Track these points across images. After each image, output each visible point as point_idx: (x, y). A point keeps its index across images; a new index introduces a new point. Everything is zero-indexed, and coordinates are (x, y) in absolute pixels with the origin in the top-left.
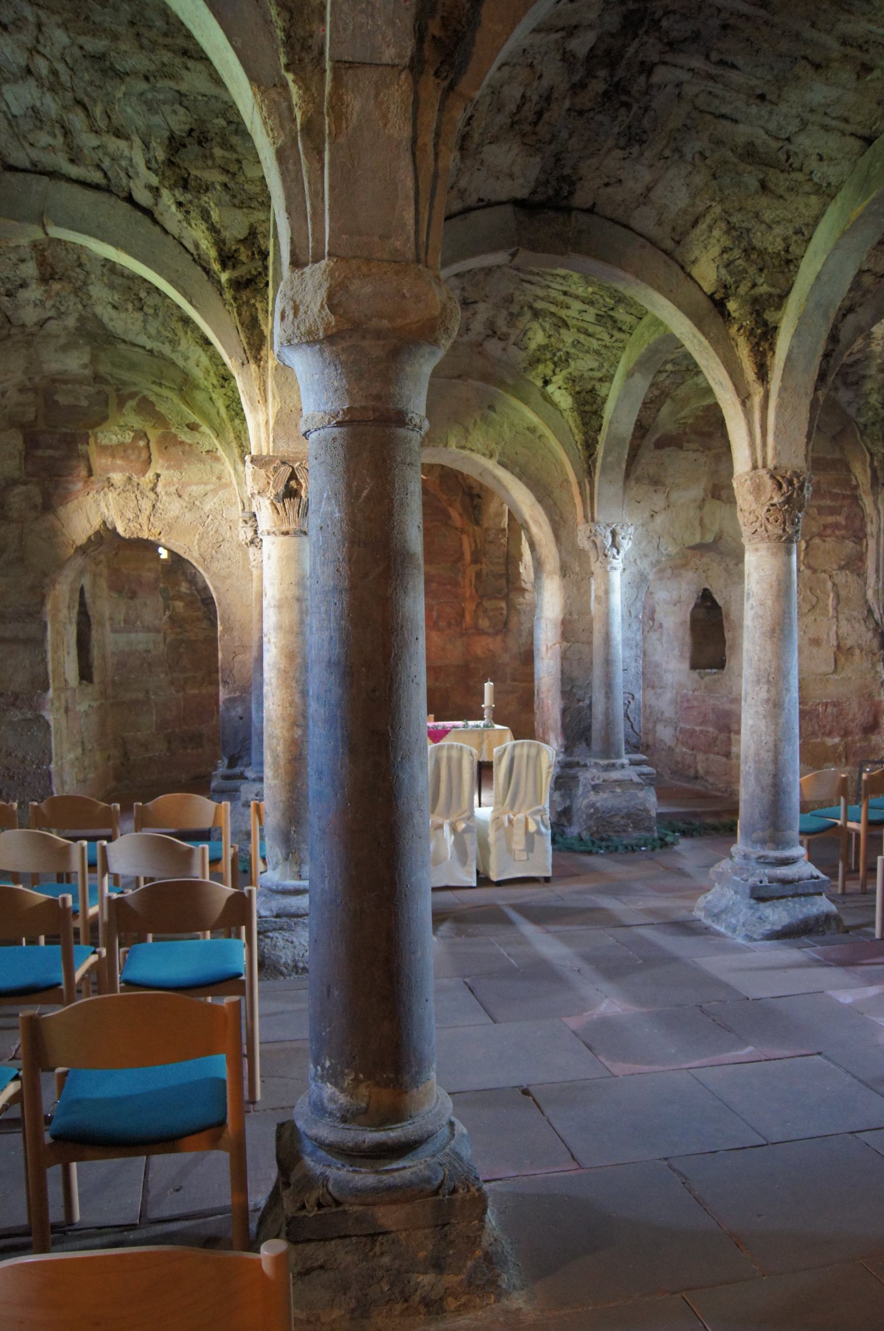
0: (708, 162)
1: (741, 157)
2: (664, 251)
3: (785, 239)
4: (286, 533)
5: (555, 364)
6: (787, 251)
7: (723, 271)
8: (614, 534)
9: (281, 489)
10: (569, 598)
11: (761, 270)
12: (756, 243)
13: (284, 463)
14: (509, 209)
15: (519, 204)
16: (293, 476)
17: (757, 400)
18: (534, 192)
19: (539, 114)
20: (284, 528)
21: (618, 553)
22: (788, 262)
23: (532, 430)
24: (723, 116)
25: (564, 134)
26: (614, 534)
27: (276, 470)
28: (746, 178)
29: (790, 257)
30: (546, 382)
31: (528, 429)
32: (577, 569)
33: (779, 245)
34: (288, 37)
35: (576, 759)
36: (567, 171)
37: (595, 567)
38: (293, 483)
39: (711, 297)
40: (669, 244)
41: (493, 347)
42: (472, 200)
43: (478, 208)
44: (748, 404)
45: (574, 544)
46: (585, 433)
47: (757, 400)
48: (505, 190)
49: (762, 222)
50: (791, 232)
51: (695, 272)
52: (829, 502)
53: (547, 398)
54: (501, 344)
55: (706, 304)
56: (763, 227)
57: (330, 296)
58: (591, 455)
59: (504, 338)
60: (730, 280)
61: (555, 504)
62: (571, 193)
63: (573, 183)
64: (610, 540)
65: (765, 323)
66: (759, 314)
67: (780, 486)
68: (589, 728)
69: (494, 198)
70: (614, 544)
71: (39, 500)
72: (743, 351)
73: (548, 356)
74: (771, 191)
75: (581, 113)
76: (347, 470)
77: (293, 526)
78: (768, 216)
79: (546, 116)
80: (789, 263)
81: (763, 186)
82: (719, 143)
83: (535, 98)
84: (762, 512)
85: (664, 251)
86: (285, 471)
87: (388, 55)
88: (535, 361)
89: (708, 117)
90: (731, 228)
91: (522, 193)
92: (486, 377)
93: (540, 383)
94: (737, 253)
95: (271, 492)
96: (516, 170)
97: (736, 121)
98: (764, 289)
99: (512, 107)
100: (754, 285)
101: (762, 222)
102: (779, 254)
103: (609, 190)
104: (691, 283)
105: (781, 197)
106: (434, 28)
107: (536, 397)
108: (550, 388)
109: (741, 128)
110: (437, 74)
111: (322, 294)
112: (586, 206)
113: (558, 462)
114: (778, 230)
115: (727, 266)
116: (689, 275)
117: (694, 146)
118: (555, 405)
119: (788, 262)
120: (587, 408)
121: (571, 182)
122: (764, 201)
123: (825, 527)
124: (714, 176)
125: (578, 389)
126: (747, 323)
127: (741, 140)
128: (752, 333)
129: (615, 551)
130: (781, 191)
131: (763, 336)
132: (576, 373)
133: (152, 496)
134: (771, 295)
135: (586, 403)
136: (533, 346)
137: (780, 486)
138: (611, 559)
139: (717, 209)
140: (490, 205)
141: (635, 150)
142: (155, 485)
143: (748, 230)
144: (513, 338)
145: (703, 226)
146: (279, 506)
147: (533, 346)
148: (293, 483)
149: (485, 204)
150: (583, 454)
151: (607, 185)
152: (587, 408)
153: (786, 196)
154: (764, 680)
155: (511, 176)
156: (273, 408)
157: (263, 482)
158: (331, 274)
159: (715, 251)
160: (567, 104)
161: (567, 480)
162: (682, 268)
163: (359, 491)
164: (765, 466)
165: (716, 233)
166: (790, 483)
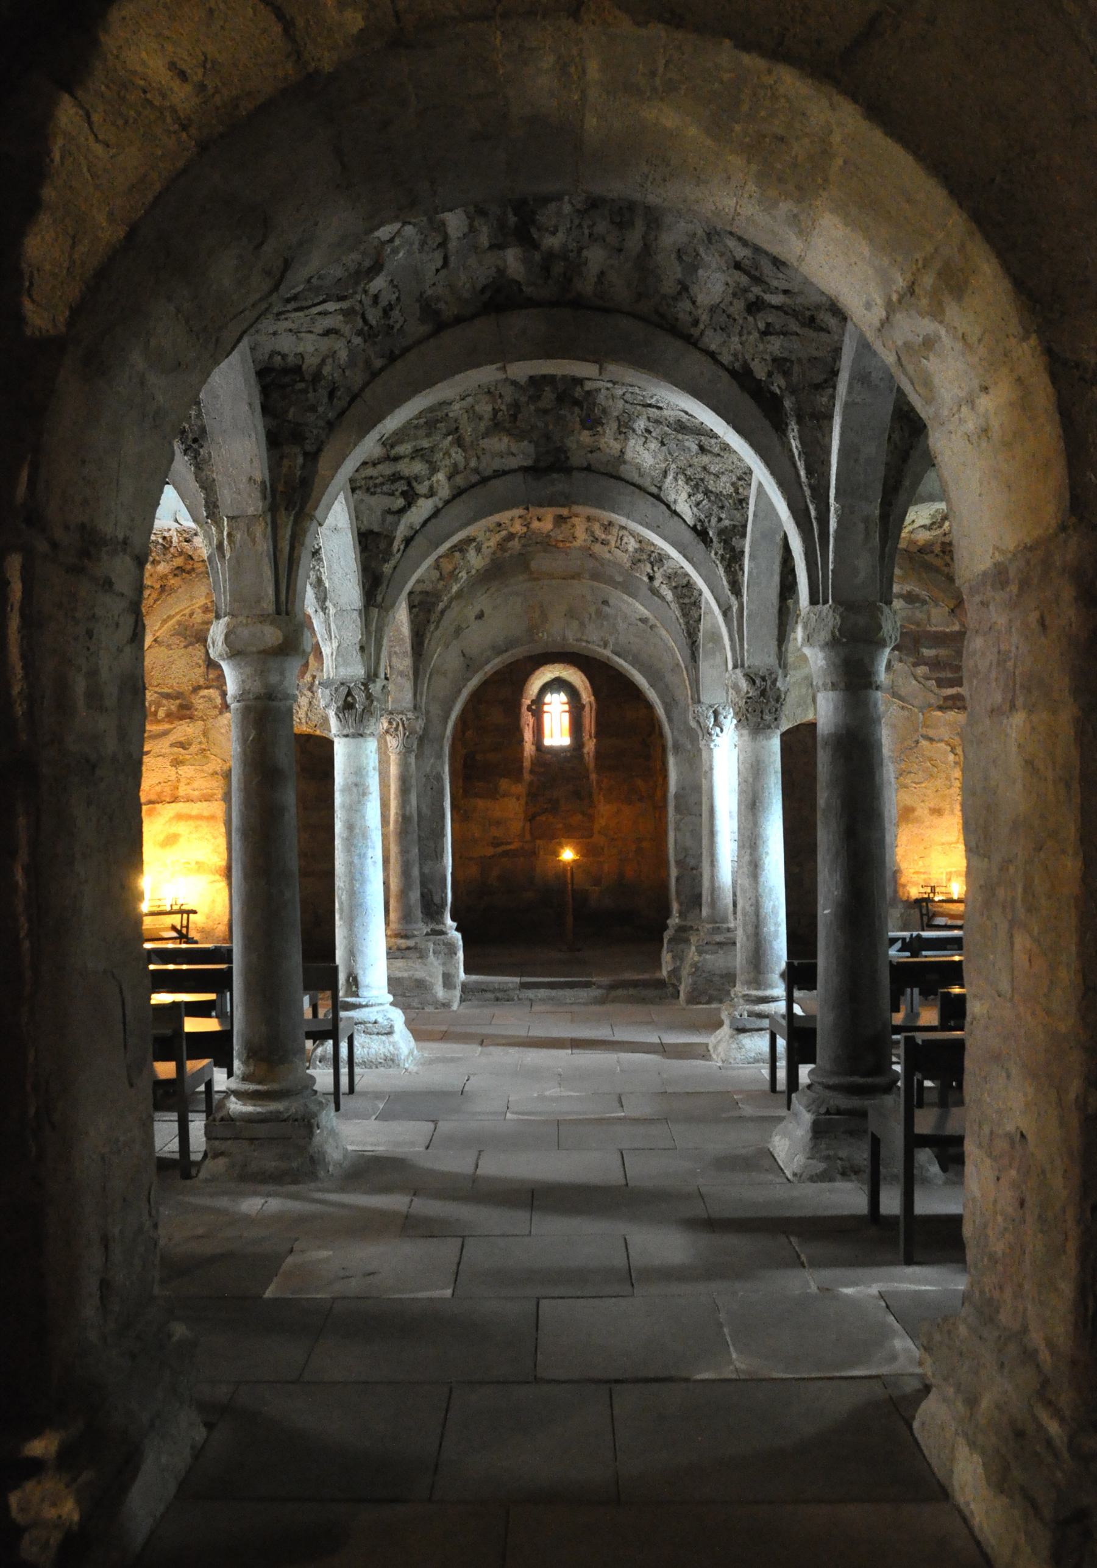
0: (654, 434)
1: (675, 430)
2: (652, 495)
3: (733, 484)
4: (346, 736)
5: (651, 563)
6: (738, 493)
7: (695, 509)
8: (716, 714)
9: (340, 703)
10: (681, 773)
11: (722, 507)
12: (710, 487)
13: (342, 684)
14: (519, 477)
15: (525, 470)
16: (349, 694)
17: (735, 609)
18: (537, 460)
19: (514, 417)
20: (345, 732)
21: (722, 730)
22: (741, 501)
23: (644, 621)
24: (650, 406)
25: (540, 424)
26: (716, 714)
27: (336, 689)
28: (687, 444)
29: (741, 497)
30: (651, 578)
31: (640, 620)
32: (689, 747)
33: (732, 490)
34: (206, 502)
35: (689, 924)
36: (559, 444)
37: (702, 743)
38: (349, 699)
39: (694, 528)
40: (654, 490)
41: (597, 548)
42: (489, 472)
43: (494, 477)
44: (729, 613)
45: (686, 723)
46: (687, 623)
47: (735, 609)
48: (513, 463)
49: (710, 473)
50: (734, 479)
51: (678, 510)
52: (950, 675)
53: (655, 592)
54: (606, 548)
55: (689, 536)
56: (712, 477)
57: (227, 636)
58: (694, 643)
59: (604, 543)
60: (702, 516)
61: (667, 686)
62: (568, 458)
63: (565, 452)
64: (712, 720)
65: (733, 549)
66: (726, 542)
67: (754, 683)
68: (700, 896)
69: (506, 468)
70: (717, 723)
71: (219, 701)
72: (721, 571)
73: (645, 557)
74: (710, 452)
75: (546, 412)
76: (242, 726)
77: (352, 730)
78: (714, 469)
79: (520, 416)
80: (743, 502)
81: (702, 449)
82: (657, 422)
83: (504, 407)
84: (742, 703)
85: (652, 495)
86: (344, 691)
87: (251, 511)
88: (636, 562)
89: (638, 408)
90: (688, 479)
91: (529, 462)
92: (596, 576)
93: (646, 579)
94: (700, 496)
95: (334, 706)
96: (514, 450)
97: (660, 408)
98: (727, 523)
99: (487, 416)
100: (720, 520)
101: (710, 473)
102: (731, 495)
103: (594, 455)
104: (676, 518)
105: (719, 455)
106: (280, 488)
107: (644, 591)
108: (656, 583)
109: (665, 412)
110: (286, 509)
111: (223, 637)
112: (585, 465)
113: (669, 649)
114: (724, 478)
115: (698, 504)
116: (675, 513)
117: (640, 424)
118: (662, 598)
119: (741, 501)
120: (686, 601)
121: (562, 450)
122: (705, 459)
123: (946, 698)
124: (663, 444)
125: (674, 584)
126: (721, 552)
127: (671, 420)
128: (723, 558)
129: (718, 729)
130: (716, 450)
131: (733, 560)
132: (670, 571)
133: (309, 694)
134: (734, 526)
135: (683, 596)
136: (631, 549)
137: (754, 683)
138: (714, 737)
139: (673, 466)
140: (505, 473)
141: (599, 429)
142: (312, 684)
143: (702, 480)
144: (613, 544)
145: (670, 477)
146: (341, 715)
147: (631, 549)
148: (349, 699)
149: (499, 474)
150: (683, 640)
151: (591, 452)
152: (686, 601)
153: (722, 454)
154: (747, 845)
155: (513, 455)
156: (335, 645)
157: (328, 698)
158: (228, 625)
159: (684, 495)
160: (532, 408)
161: (678, 665)
162: (668, 507)
163: (249, 736)
164: (743, 666)
165: (680, 482)
166: (763, 679)
